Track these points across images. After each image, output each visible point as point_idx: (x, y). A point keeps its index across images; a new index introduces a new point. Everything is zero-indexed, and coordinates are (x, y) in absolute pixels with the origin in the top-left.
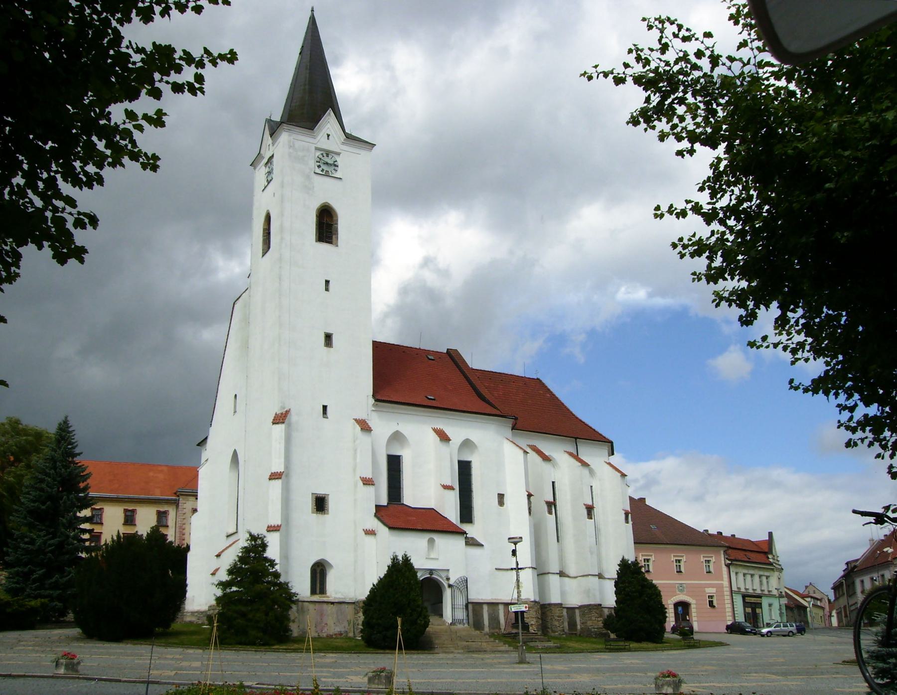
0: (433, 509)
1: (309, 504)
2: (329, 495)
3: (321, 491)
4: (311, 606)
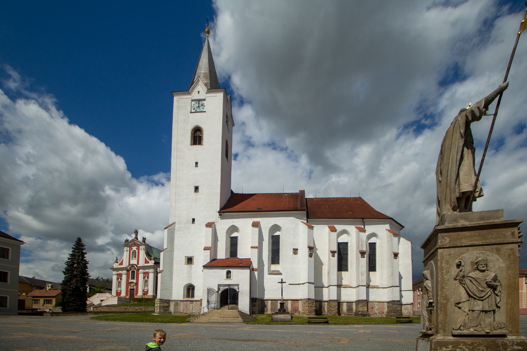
1: (184, 260)
3: (190, 255)
4: (182, 303)
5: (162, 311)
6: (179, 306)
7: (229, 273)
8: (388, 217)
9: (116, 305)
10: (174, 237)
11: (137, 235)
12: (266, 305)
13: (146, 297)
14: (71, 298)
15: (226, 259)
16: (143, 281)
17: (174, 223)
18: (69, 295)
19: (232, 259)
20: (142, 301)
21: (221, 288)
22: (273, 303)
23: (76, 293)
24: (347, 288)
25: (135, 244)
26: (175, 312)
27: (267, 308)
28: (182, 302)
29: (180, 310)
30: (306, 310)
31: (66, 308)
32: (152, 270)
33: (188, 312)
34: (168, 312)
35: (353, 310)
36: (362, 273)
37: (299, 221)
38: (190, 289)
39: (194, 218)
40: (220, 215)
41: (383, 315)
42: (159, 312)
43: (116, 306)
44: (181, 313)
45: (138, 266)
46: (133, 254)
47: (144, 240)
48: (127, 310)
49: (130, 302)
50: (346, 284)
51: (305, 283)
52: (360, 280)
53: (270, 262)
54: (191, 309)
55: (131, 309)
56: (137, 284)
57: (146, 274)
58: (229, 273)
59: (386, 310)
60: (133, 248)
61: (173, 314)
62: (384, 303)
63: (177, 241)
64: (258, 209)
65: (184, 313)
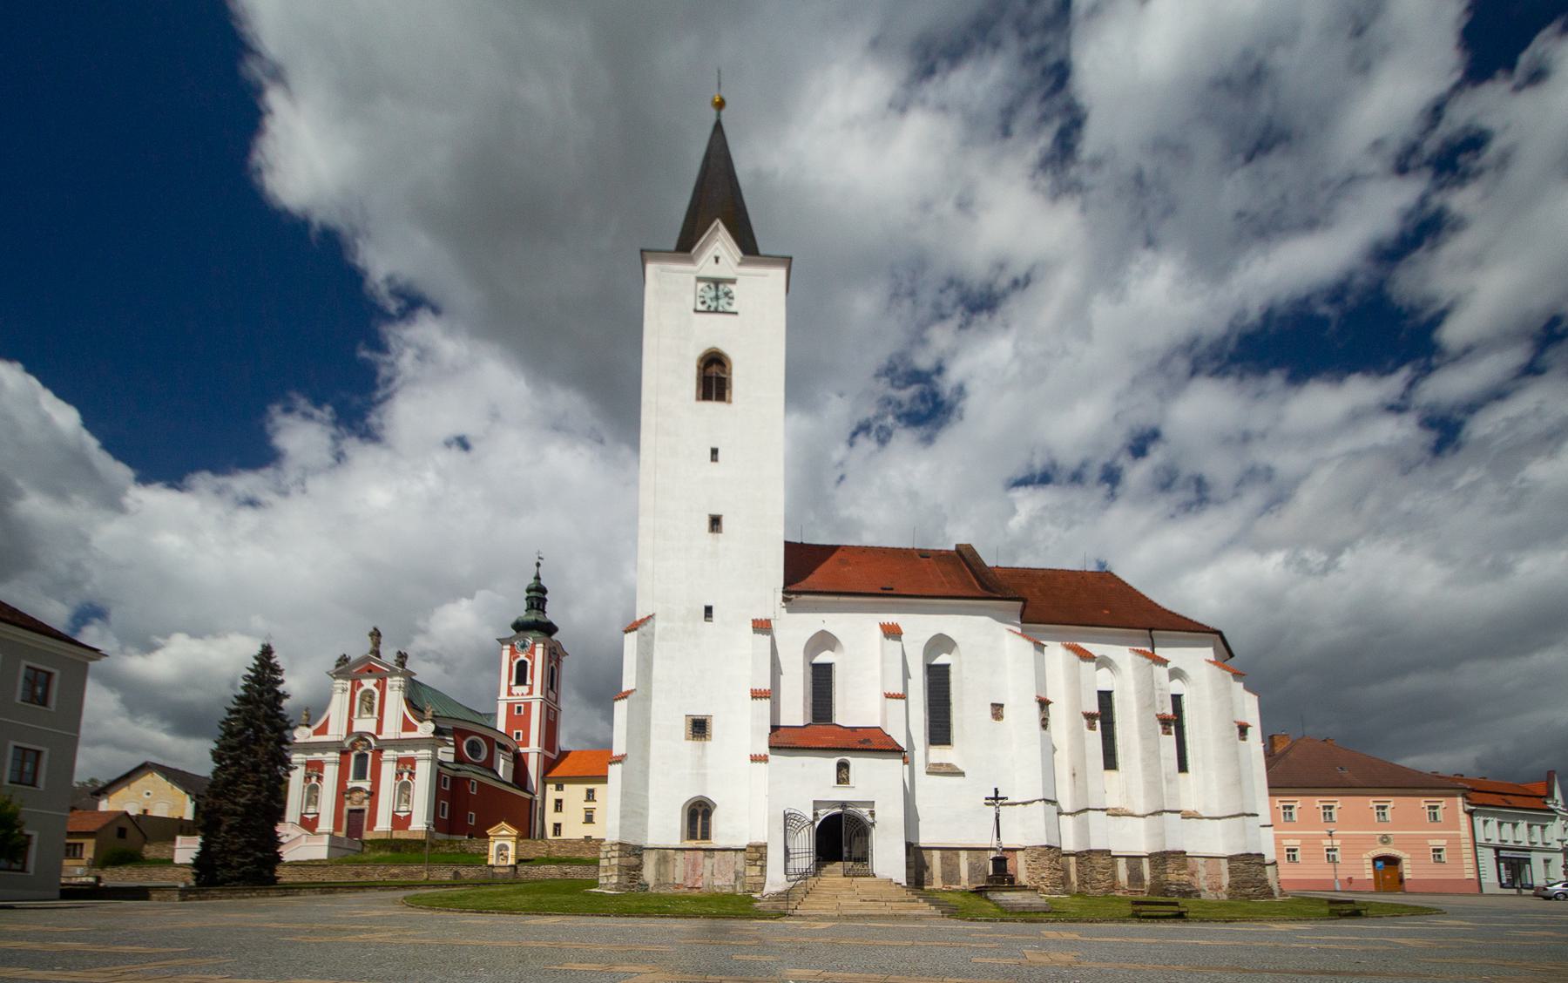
0: (879, 728)
1: (682, 727)
3: (699, 712)
4: (680, 856)
5: (625, 879)
7: (843, 767)
8: (1209, 628)
9: (324, 860)
10: (652, 655)
11: (379, 643)
12: (928, 864)
13: (401, 835)
14: (236, 841)
15: (805, 726)
16: (395, 784)
18: (231, 828)
19: (821, 727)
20: (402, 849)
23: (253, 824)
25: (370, 671)
26: (659, 884)
27: (932, 874)
28: (679, 853)
29: (675, 878)
30: (1043, 878)
31: (218, 873)
32: (426, 751)
33: (699, 884)
35: (1144, 880)
36: (1169, 777)
37: (1002, 628)
38: (699, 814)
39: (709, 604)
40: (785, 600)
41: (1219, 895)
43: (325, 866)
44: (678, 886)
45: (379, 737)
46: (362, 700)
47: (401, 660)
48: (363, 878)
49: (362, 850)
51: (1034, 801)
52: (1165, 797)
53: (928, 744)
54: (707, 874)
55: (376, 876)
56: (373, 794)
57: (407, 765)
58: (843, 767)
59: (1225, 880)
60: (363, 681)
61: (652, 889)
63: (658, 671)
65: (686, 887)
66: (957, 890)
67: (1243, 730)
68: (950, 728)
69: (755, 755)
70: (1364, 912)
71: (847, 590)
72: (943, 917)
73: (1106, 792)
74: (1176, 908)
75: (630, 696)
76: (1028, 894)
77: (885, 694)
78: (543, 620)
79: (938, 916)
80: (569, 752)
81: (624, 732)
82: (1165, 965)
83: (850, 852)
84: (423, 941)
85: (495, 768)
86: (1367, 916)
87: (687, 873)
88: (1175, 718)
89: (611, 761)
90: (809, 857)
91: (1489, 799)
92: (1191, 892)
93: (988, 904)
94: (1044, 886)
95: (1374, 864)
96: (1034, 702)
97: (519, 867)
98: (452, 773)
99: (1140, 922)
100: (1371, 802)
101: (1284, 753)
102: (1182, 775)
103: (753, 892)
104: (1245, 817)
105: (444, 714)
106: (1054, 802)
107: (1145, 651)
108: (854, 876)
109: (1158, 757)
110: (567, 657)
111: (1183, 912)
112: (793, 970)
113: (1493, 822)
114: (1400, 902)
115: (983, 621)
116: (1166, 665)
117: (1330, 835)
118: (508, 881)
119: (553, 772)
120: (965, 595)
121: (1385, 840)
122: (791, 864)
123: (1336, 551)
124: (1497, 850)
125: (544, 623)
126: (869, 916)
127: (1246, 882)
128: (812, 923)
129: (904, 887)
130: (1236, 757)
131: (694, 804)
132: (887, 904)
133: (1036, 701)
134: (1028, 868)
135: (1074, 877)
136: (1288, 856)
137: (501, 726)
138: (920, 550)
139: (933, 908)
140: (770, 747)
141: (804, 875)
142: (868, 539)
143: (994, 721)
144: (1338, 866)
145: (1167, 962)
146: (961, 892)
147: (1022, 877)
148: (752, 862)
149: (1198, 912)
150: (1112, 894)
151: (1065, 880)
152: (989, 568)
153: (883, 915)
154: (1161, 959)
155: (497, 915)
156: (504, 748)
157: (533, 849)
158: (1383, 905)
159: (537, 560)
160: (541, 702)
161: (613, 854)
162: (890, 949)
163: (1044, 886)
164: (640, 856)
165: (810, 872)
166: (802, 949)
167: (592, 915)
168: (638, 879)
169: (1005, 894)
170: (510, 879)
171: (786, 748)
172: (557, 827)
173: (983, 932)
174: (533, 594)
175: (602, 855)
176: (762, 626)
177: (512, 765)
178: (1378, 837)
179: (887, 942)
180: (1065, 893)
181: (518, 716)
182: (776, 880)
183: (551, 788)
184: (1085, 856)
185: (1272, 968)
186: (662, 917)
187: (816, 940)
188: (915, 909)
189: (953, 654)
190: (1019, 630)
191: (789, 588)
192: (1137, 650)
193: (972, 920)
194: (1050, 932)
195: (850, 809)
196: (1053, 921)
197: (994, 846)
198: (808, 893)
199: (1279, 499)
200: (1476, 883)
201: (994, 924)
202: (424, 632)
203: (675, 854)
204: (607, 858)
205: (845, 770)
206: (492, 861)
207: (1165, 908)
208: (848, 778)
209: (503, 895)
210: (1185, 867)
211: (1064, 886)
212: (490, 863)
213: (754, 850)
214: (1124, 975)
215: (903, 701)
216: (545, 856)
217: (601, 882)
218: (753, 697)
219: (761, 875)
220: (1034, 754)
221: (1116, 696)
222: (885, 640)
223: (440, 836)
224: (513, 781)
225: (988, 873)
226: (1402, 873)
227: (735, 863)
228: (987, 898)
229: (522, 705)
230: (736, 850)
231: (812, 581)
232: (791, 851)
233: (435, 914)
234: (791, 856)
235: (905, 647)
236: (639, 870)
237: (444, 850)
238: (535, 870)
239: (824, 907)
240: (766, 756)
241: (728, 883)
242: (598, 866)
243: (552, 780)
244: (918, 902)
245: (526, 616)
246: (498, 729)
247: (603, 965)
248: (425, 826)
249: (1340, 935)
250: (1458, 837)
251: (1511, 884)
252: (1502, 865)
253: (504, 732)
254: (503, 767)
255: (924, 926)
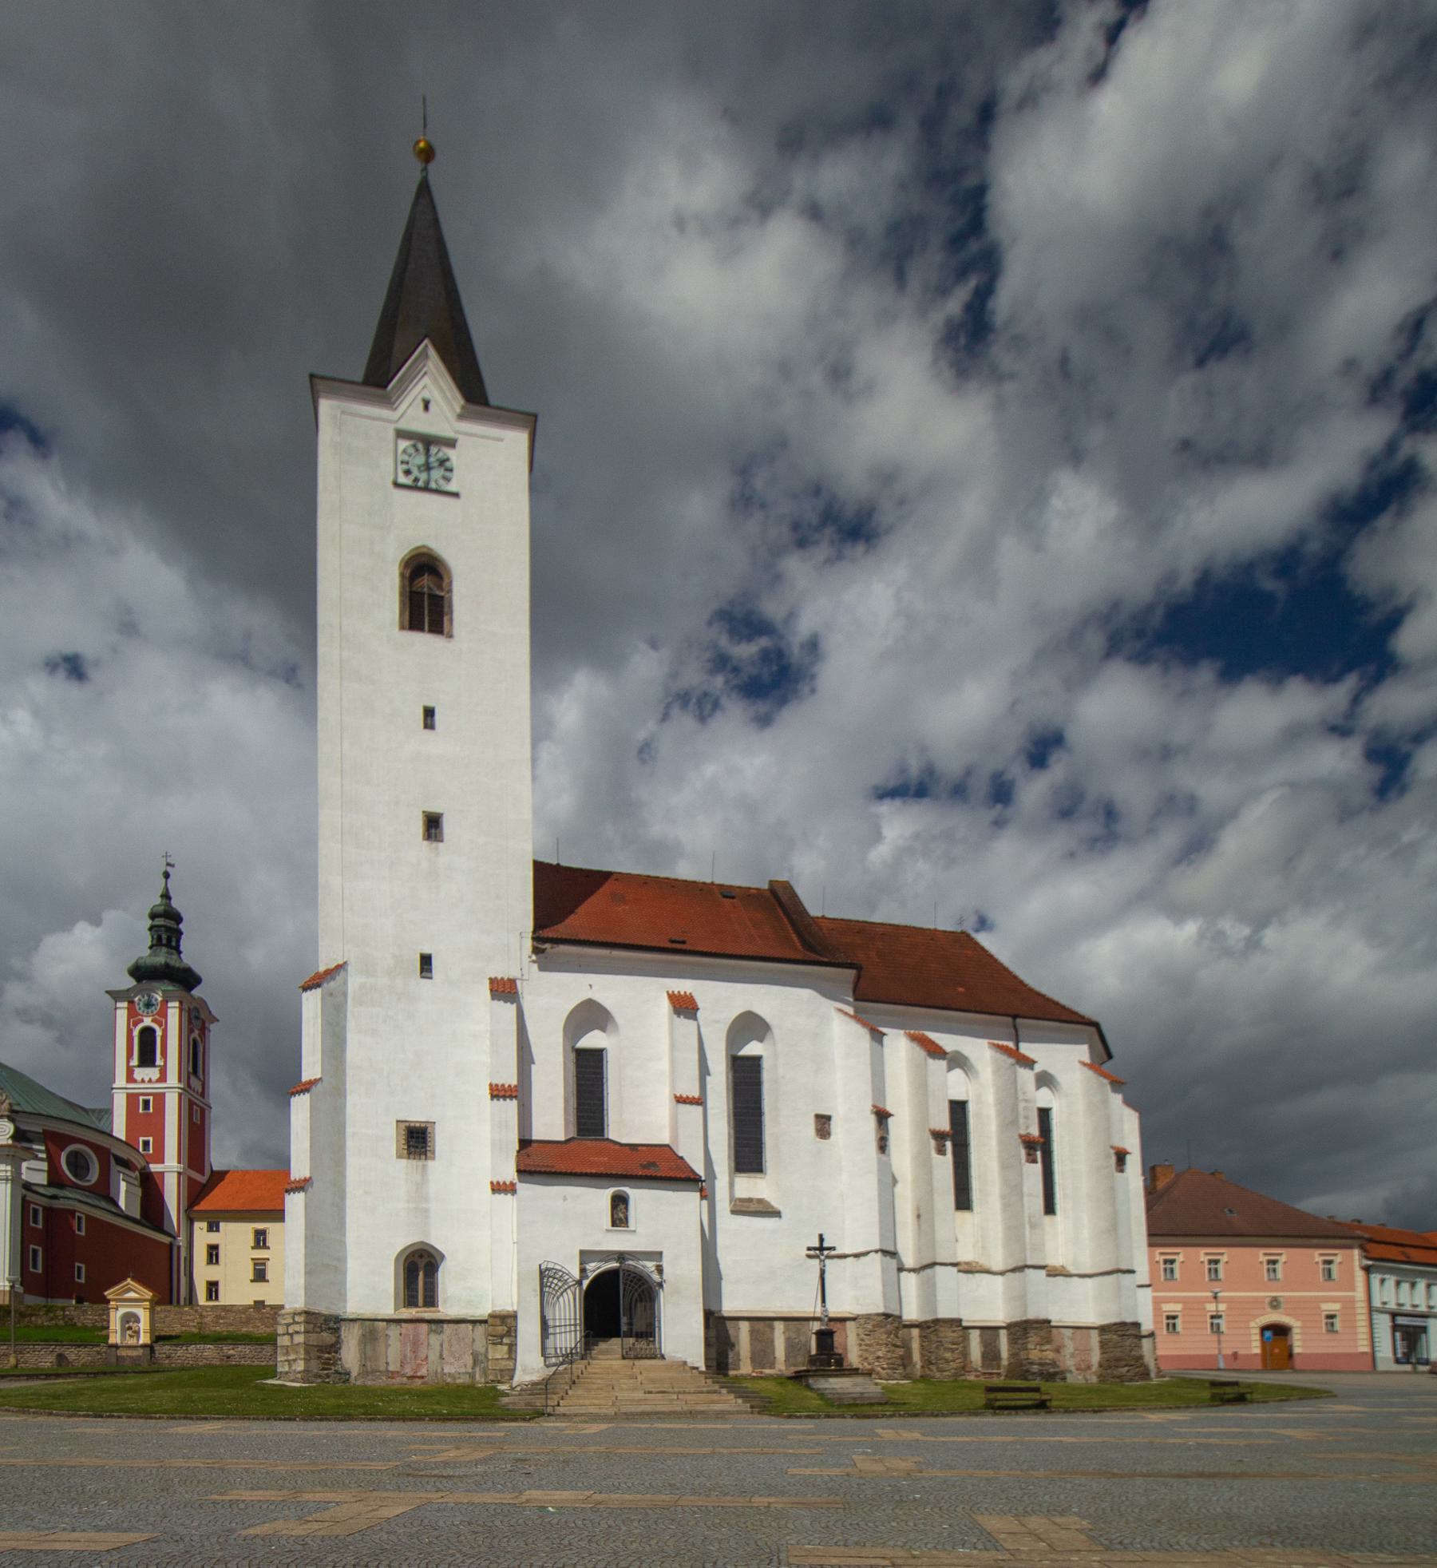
0: (668, 1146)
1: (391, 1140)
2: (434, 1123)
4: (394, 1332)
5: (315, 1366)
6: (381, 1348)
10: (344, 1027)
12: (733, 1339)
15: (567, 1141)
17: (341, 967)
19: (589, 1143)
21: (591, 1266)
22: (758, 1331)
24: (977, 1275)
26: (365, 1372)
27: (738, 1354)
28: (393, 1326)
29: (387, 1363)
33: (423, 1372)
34: (337, 1372)
36: (1033, 1220)
37: (829, 1007)
39: (427, 951)
41: (1088, 1377)
42: (304, 1371)
44: (392, 1375)
50: (967, 1260)
52: (1028, 1247)
53: (733, 1169)
54: (433, 1356)
59: (1096, 1357)
62: (1092, 1331)
63: (355, 1050)
64: (673, 942)
66: (771, 1375)
67: (1121, 1157)
68: (761, 1148)
69: (498, 1183)
70: (1248, 1396)
71: (623, 941)
72: (752, 1413)
73: (957, 1241)
74: (1037, 1396)
75: (314, 1089)
76: (860, 1380)
77: (676, 1097)
78: (177, 965)
79: (746, 1412)
80: (226, 1172)
81: (307, 1144)
82: (1021, 1471)
83: (630, 1324)
84: (12, 1461)
85: (111, 1195)
86: (1252, 1402)
87: (405, 1356)
88: (1042, 1140)
89: (289, 1187)
90: (575, 1331)
91: (1393, 1252)
92: (1056, 1374)
93: (809, 1394)
94: (879, 1369)
95: (1262, 1335)
96: (869, 1112)
97: (157, 1347)
98: (45, 1202)
99: (995, 1414)
100: (1261, 1255)
101: (1168, 1189)
102: (1048, 1219)
103: (499, 1382)
104: (1120, 1274)
105: (29, 1109)
106: (893, 1254)
107: (1007, 1047)
108: (637, 1358)
109: (1021, 1194)
110: (216, 1024)
111: (1046, 1400)
112: (553, 1492)
113: (1391, 1280)
114: (1288, 1383)
115: (806, 994)
116: (1032, 1068)
117: (1215, 1297)
118: (140, 1369)
119: (202, 1203)
120: (777, 955)
121: (1275, 1303)
122: (550, 1342)
123: (1261, 921)
124: (1394, 1315)
125: (178, 969)
126: (656, 1413)
127: (1118, 1360)
128: (579, 1425)
129: (701, 1372)
130: (1112, 1195)
131: (413, 1254)
132: (681, 1396)
133: (872, 1112)
134: (860, 1345)
135: (916, 1356)
136: (1168, 1325)
137: (120, 1130)
138: (721, 886)
139: (740, 1401)
140: (519, 1171)
141: (569, 1358)
142: (685, 871)
143: (818, 1139)
144: (1223, 1338)
145: (1025, 1466)
146: (776, 1378)
147: (853, 1358)
148: (496, 1339)
149: (1063, 1399)
150: (963, 1378)
151: (906, 1360)
152: (813, 918)
153: (674, 1412)
154: (1017, 1462)
155: (125, 1420)
156: (126, 1164)
157: (177, 1321)
158: (1270, 1387)
159: (163, 868)
160: (180, 1095)
161: (297, 1328)
162: (683, 1459)
163: (879, 1369)
164: (336, 1331)
165: (577, 1353)
166: (566, 1462)
167: (268, 1419)
168: (334, 1364)
169: (832, 1380)
170: (145, 1365)
171: (540, 1173)
172: (213, 1288)
173: (803, 1432)
174: (159, 922)
175: (280, 1330)
176: (504, 990)
177: (139, 1191)
178: (1267, 1300)
179: (679, 1450)
180: (905, 1377)
181: (145, 1113)
182: (530, 1365)
183: (200, 1227)
184: (930, 1327)
185: (1144, 1470)
186: (370, 1420)
187: (585, 1450)
188: (717, 1402)
189: (766, 1041)
190: (851, 1011)
191: (541, 933)
192: (994, 1044)
193: (789, 1417)
194: (887, 1430)
195: (631, 1262)
196: (891, 1416)
197: (818, 1315)
198: (574, 1383)
199: (1198, 846)
200: (1369, 1359)
201: (817, 1421)
202: (22, 977)
203: (387, 1329)
204: (288, 1334)
205: (622, 1207)
206: (115, 1338)
207: (1024, 1395)
208: (626, 1218)
209: (133, 1389)
210: (1049, 1341)
211: (905, 1368)
212: (112, 1340)
213: (498, 1321)
214: (973, 1485)
215: (700, 1109)
216: (195, 1330)
217: (280, 1369)
218: (493, 1097)
219: (509, 1359)
220: (869, 1186)
221: (972, 1109)
222: (675, 1016)
223: (32, 1300)
224: (141, 1215)
225: (809, 1351)
226: (1290, 1347)
227: (474, 1340)
228: (808, 1387)
229: (151, 1098)
230: (474, 1322)
231: (572, 924)
232: (551, 1323)
233: (31, 1419)
234: (551, 1330)
235: (702, 1030)
236: (336, 1352)
237: (40, 1322)
238: (181, 1352)
239: (596, 1402)
240: (513, 1185)
241: (463, 1370)
242: (275, 1344)
243: (204, 1216)
244: (720, 1393)
245: (150, 955)
246: (114, 1134)
247: (285, 1492)
248: (7, 1283)
249: (1222, 1427)
250: (1352, 1300)
251: (1405, 1359)
252: (1398, 1335)
253: (123, 1138)
254: (125, 1193)
255: (728, 1426)
